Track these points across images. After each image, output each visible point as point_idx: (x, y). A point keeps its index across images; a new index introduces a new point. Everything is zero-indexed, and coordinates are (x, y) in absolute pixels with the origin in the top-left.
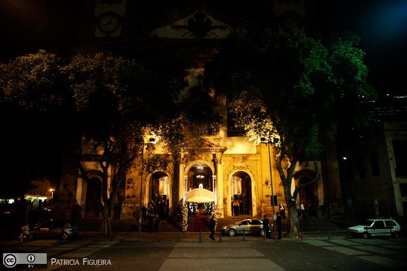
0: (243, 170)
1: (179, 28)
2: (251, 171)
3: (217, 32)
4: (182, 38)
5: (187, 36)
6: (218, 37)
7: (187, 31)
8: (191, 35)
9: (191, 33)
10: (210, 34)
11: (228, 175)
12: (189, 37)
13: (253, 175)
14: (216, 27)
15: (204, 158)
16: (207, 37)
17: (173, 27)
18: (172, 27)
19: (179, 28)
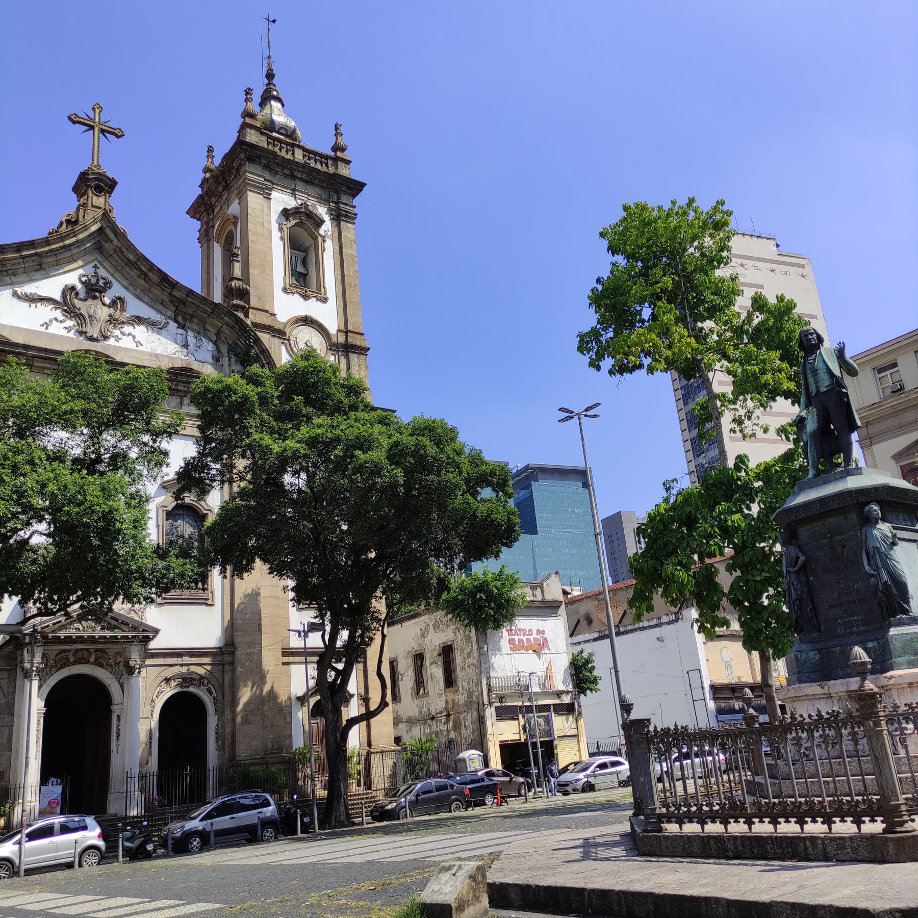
0: (192, 689)
1: (33, 299)
2: (209, 691)
3: (140, 331)
4: (43, 329)
5: (57, 329)
6: (140, 348)
7: (58, 314)
8: (69, 329)
9: (70, 323)
10: (120, 336)
11: (153, 701)
12: (64, 333)
13: (214, 698)
14: (138, 320)
15: (92, 659)
16: (111, 342)
17: (19, 297)
18: (15, 294)
19: (33, 299)
